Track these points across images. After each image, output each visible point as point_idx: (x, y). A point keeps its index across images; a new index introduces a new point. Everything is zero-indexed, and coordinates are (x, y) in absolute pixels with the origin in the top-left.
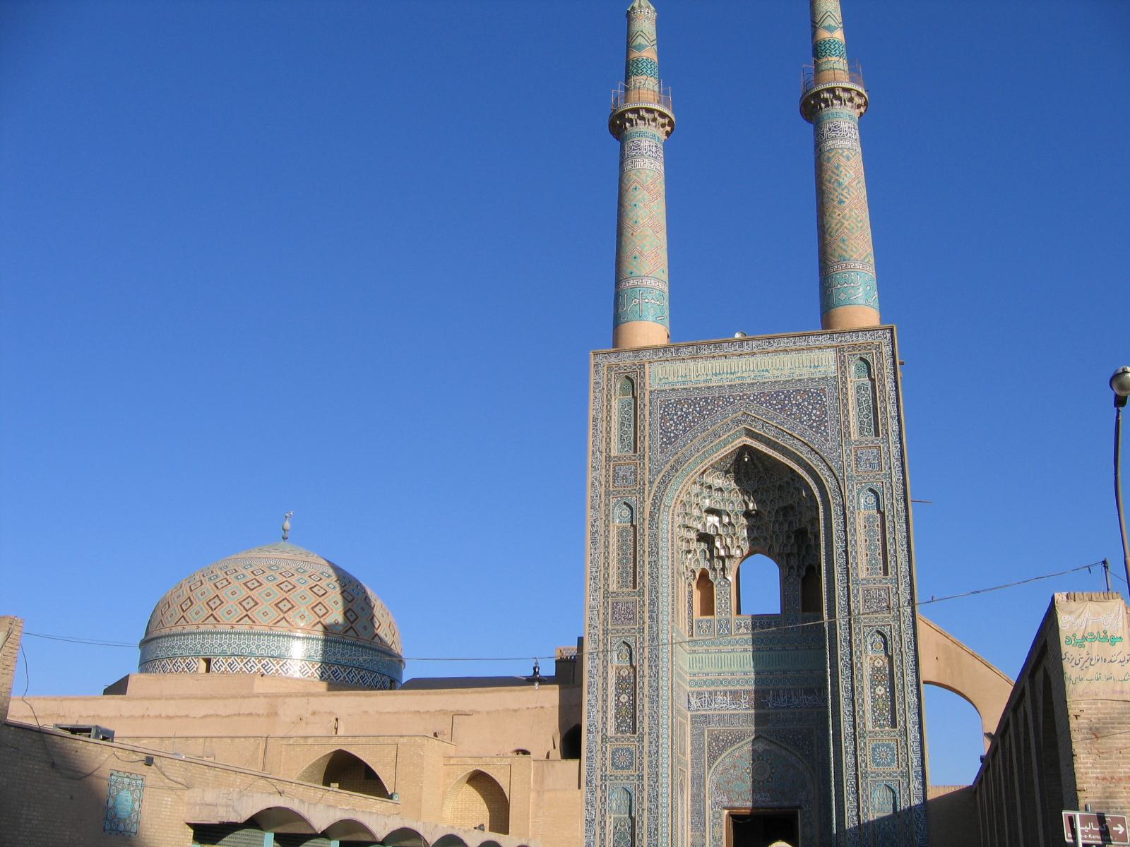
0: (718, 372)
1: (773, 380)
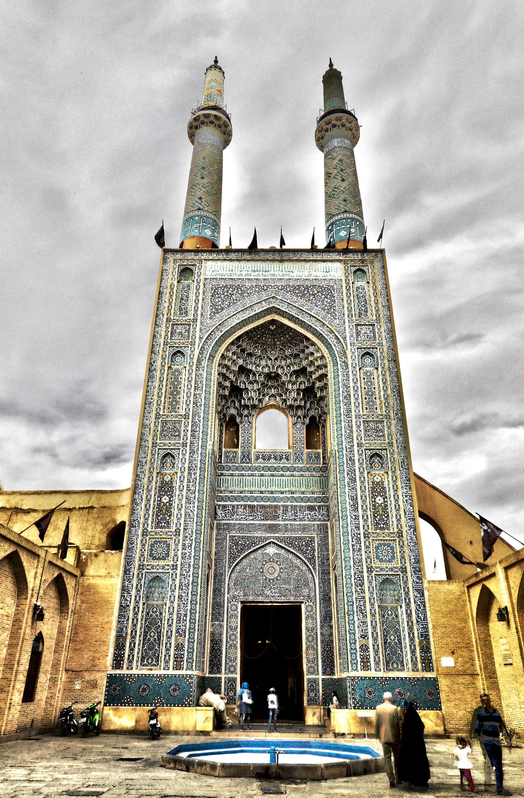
0: (256, 270)
1: (296, 278)
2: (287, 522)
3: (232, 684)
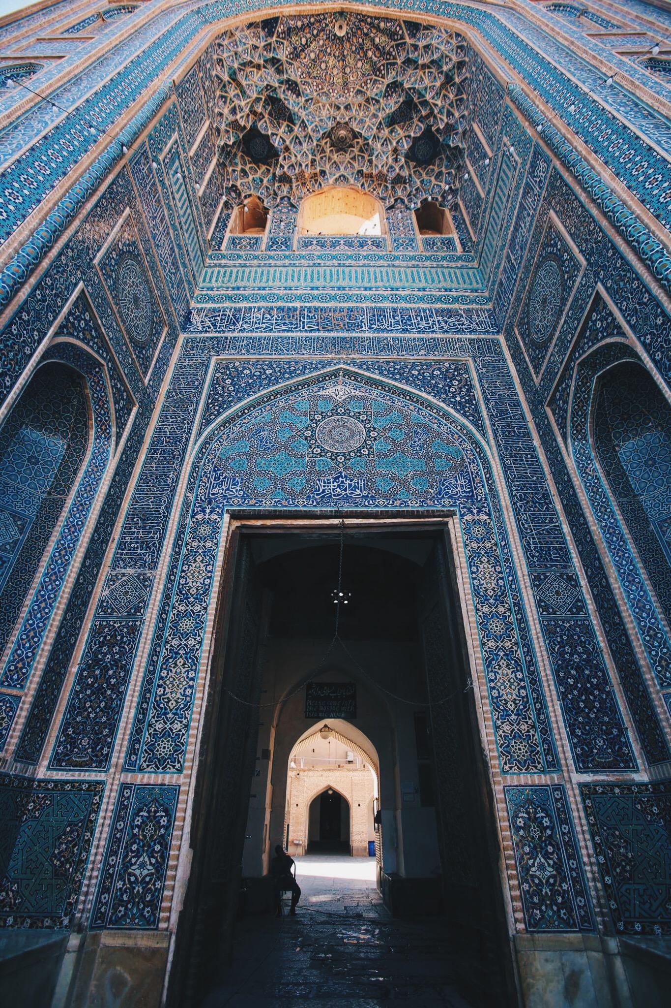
2: (385, 335)
3: (153, 818)
